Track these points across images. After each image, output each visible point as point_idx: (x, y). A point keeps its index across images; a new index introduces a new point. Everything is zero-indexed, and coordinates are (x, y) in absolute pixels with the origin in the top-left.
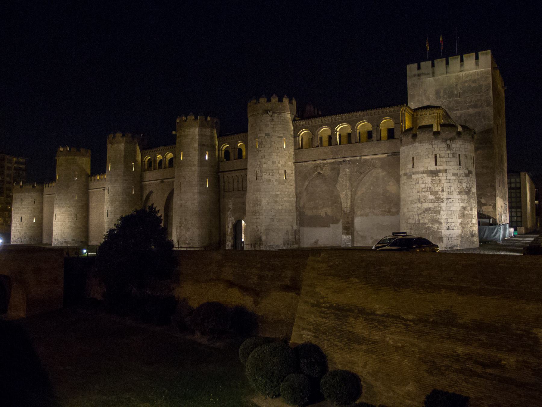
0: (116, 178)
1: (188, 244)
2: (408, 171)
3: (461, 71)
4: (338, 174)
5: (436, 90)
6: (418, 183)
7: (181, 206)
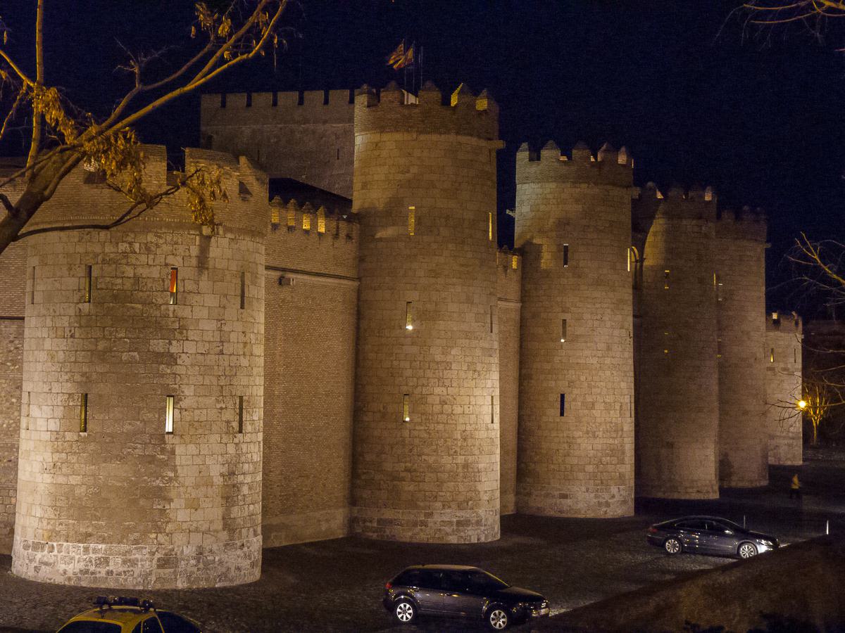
2: (789, 366)
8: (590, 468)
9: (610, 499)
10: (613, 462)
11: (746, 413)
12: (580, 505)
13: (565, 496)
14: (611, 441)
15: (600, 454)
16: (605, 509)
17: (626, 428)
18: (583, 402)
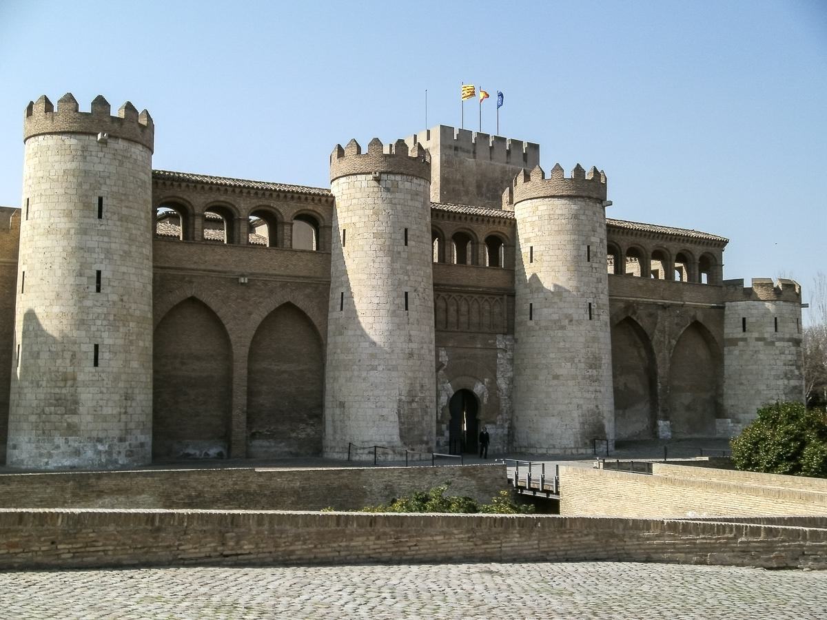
0: (126, 247)
1: (427, 443)
2: (766, 336)
3: (507, 163)
4: (656, 324)
5: (477, 182)
6: (783, 353)
7: (411, 355)
8: (33, 418)
9: (53, 450)
10: (59, 412)
11: (556, 377)
12: (24, 456)
13: (15, 447)
14: (57, 390)
15: (42, 404)
16: (46, 460)
17: (80, 377)
18: (30, 352)
